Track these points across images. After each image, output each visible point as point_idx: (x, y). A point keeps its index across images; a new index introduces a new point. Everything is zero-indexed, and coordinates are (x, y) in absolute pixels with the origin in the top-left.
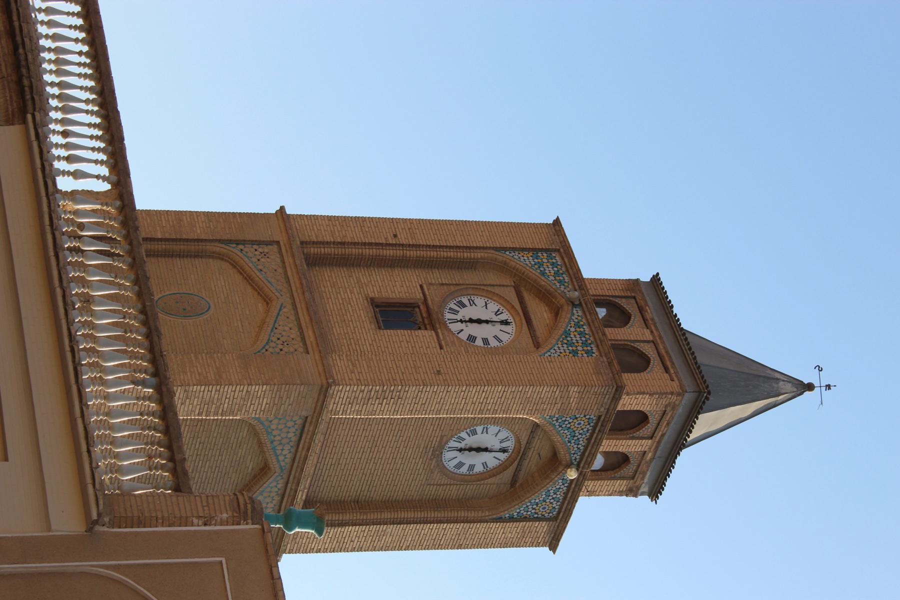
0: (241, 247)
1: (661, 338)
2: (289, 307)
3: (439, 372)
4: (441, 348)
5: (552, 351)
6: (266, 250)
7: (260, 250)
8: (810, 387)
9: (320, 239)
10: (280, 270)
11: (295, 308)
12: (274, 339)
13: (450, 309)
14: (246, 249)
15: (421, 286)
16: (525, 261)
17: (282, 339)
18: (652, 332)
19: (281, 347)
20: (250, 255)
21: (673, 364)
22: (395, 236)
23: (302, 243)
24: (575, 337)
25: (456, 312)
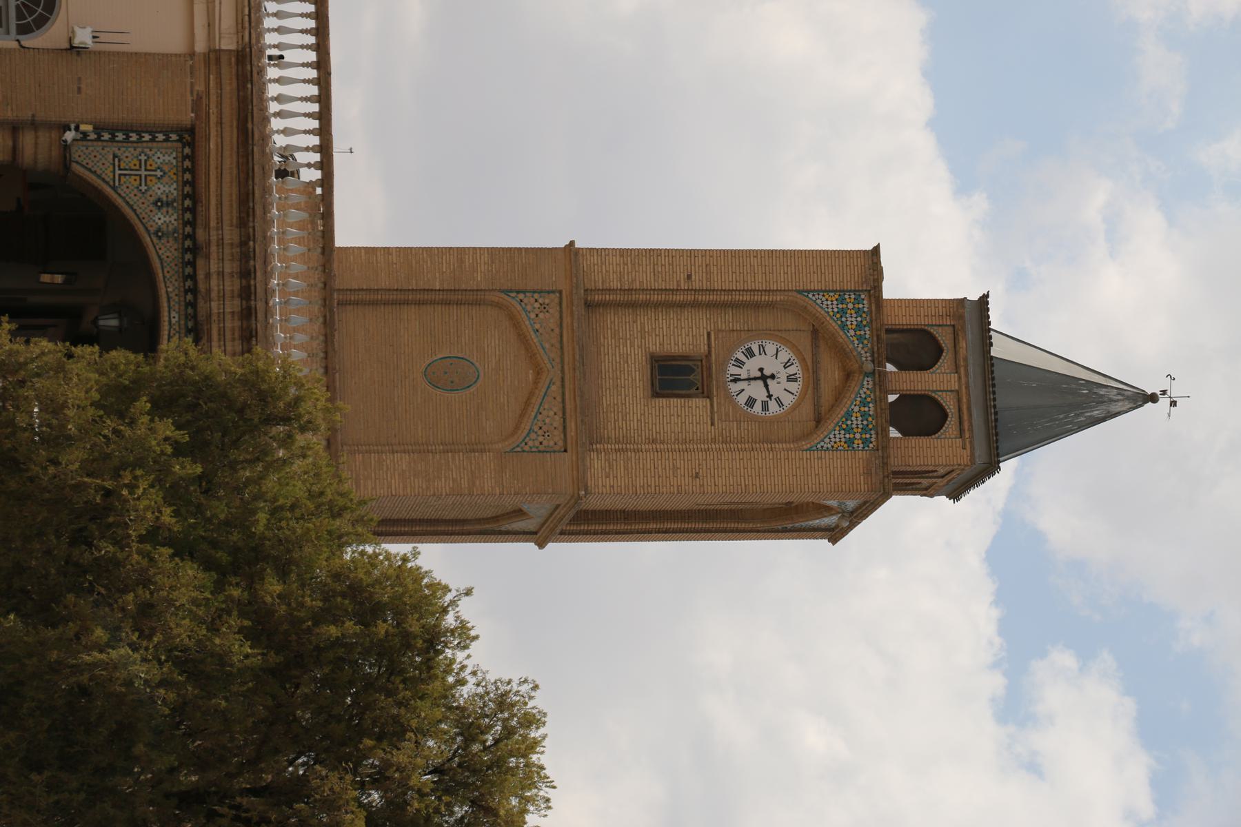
0: (521, 296)
1: (967, 387)
2: (559, 383)
3: (697, 477)
4: (712, 424)
5: (827, 440)
6: (547, 301)
7: (541, 301)
8: (1153, 398)
9: (607, 286)
10: (557, 331)
11: (563, 386)
12: (536, 428)
13: (737, 360)
14: (526, 301)
15: (709, 334)
16: (827, 306)
17: (545, 428)
18: (960, 378)
19: (541, 439)
20: (529, 308)
21: (971, 425)
22: (689, 277)
23: (586, 290)
24: (856, 421)
25: (740, 364)
